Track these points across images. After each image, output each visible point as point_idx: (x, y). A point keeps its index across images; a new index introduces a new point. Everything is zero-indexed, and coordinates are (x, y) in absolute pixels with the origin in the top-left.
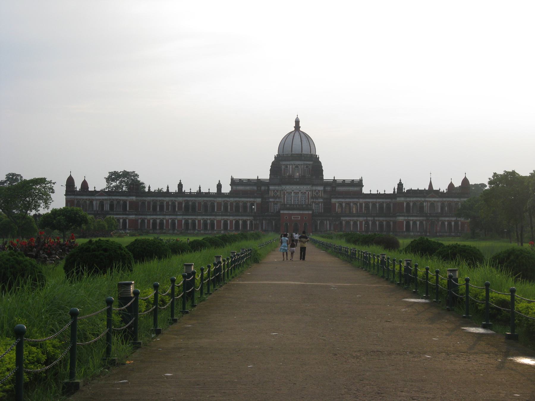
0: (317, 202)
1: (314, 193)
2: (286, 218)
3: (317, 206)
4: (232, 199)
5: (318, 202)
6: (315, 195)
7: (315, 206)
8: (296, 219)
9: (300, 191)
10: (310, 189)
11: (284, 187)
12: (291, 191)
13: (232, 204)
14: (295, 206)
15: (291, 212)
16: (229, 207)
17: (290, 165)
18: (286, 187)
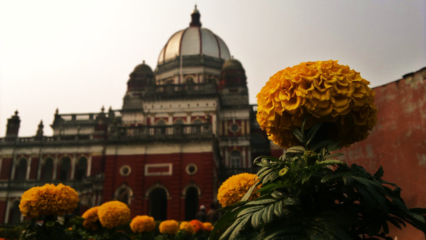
0: (235, 149)
1: (226, 127)
2: (126, 171)
3: (235, 158)
4: (36, 151)
5: (238, 147)
6: (231, 130)
7: (232, 158)
8: (158, 174)
9: (189, 113)
10: (214, 109)
11: (148, 106)
12: (166, 115)
13: (35, 161)
14: (152, 131)
15: (140, 151)
16: (29, 169)
17: (174, 76)
18: (153, 107)
